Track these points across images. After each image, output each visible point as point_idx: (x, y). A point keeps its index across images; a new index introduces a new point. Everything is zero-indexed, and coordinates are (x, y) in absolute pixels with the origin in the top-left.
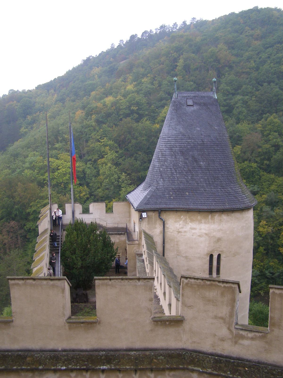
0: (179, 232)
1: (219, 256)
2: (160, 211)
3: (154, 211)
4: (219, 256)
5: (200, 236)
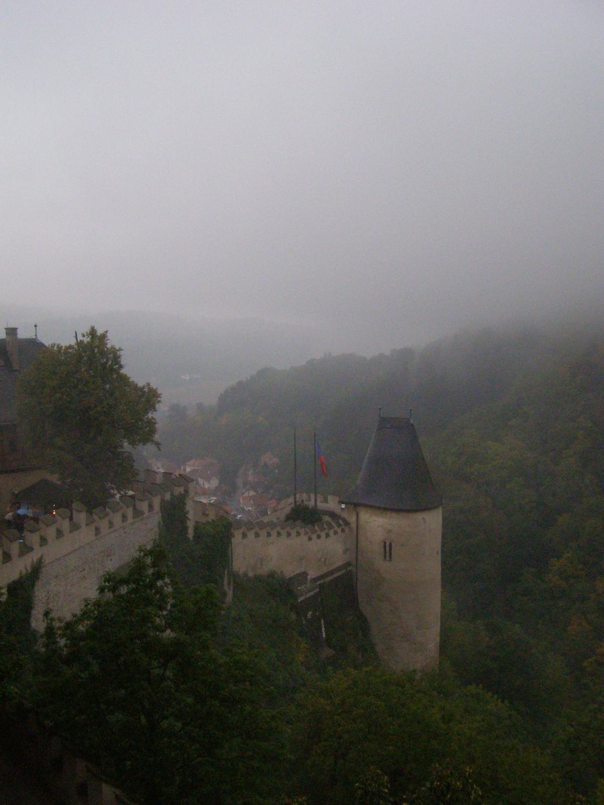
0: (367, 522)
1: (390, 544)
2: (356, 505)
3: (351, 503)
4: (390, 544)
5: (378, 527)
